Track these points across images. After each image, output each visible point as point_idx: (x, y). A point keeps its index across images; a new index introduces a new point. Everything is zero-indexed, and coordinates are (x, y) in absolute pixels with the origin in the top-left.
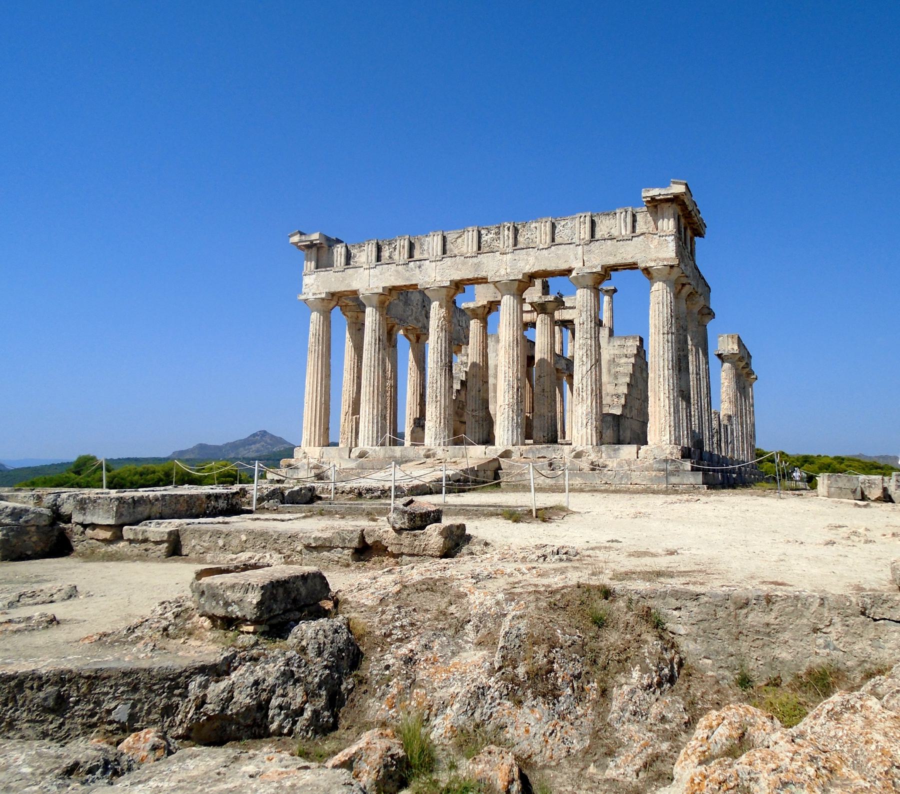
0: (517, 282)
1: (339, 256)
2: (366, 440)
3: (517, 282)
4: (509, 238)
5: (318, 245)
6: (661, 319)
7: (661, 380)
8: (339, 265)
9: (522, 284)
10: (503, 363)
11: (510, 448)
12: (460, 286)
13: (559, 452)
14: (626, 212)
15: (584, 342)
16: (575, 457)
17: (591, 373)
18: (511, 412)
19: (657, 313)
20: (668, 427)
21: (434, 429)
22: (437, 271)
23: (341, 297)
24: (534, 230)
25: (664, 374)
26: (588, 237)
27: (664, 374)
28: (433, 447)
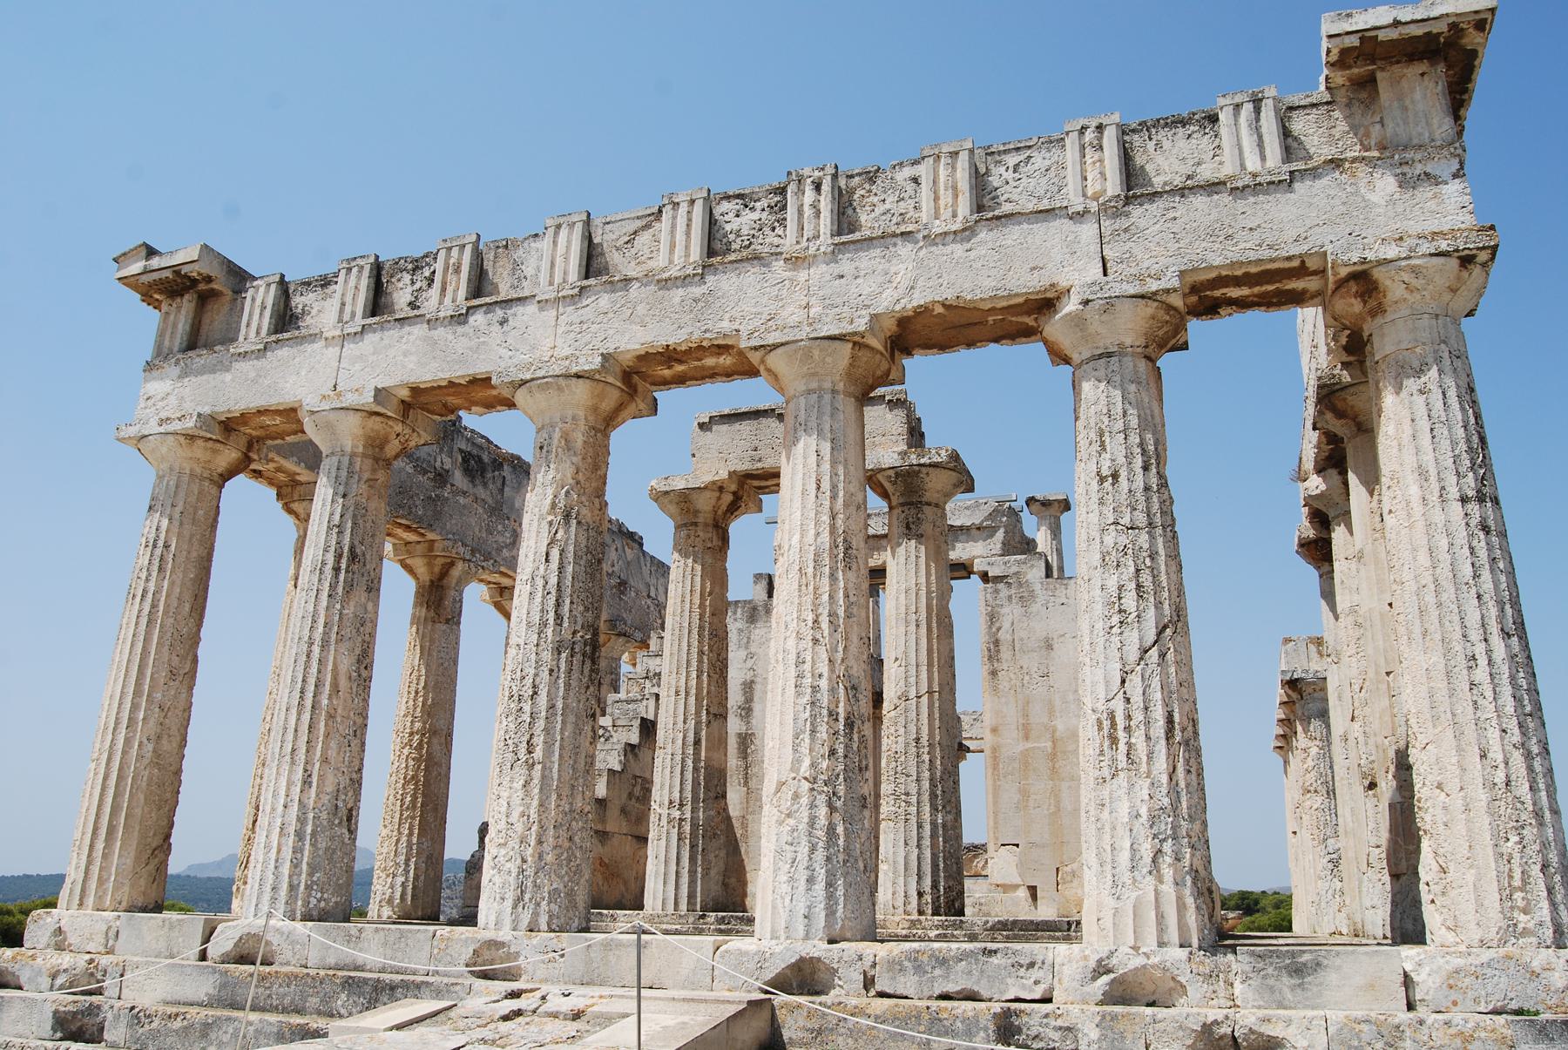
0: (850, 345)
1: (257, 311)
2: (266, 897)
3: (847, 348)
4: (818, 214)
5: (202, 287)
6: (1445, 444)
7: (1481, 674)
8: (252, 334)
9: (864, 355)
10: (793, 625)
11: (818, 948)
12: (642, 385)
13: (1035, 974)
14: (1257, 102)
15: (1123, 540)
16: (1111, 998)
17: (1163, 655)
18: (823, 811)
19: (1425, 425)
20: (1535, 870)
21: (513, 867)
22: (560, 331)
23: (260, 440)
24: (910, 187)
25: (1489, 652)
26: (1114, 186)
27: (1489, 652)
28: (505, 934)
